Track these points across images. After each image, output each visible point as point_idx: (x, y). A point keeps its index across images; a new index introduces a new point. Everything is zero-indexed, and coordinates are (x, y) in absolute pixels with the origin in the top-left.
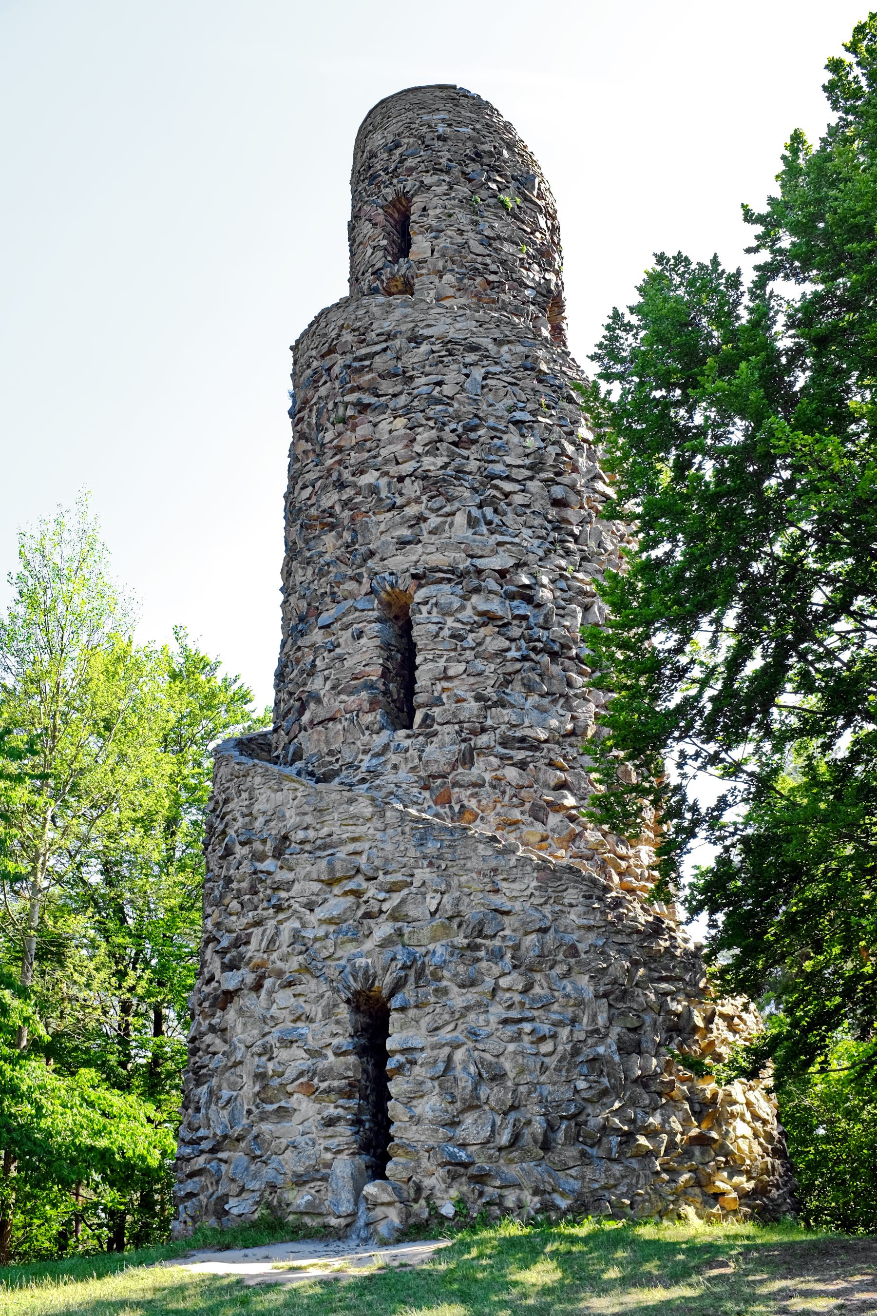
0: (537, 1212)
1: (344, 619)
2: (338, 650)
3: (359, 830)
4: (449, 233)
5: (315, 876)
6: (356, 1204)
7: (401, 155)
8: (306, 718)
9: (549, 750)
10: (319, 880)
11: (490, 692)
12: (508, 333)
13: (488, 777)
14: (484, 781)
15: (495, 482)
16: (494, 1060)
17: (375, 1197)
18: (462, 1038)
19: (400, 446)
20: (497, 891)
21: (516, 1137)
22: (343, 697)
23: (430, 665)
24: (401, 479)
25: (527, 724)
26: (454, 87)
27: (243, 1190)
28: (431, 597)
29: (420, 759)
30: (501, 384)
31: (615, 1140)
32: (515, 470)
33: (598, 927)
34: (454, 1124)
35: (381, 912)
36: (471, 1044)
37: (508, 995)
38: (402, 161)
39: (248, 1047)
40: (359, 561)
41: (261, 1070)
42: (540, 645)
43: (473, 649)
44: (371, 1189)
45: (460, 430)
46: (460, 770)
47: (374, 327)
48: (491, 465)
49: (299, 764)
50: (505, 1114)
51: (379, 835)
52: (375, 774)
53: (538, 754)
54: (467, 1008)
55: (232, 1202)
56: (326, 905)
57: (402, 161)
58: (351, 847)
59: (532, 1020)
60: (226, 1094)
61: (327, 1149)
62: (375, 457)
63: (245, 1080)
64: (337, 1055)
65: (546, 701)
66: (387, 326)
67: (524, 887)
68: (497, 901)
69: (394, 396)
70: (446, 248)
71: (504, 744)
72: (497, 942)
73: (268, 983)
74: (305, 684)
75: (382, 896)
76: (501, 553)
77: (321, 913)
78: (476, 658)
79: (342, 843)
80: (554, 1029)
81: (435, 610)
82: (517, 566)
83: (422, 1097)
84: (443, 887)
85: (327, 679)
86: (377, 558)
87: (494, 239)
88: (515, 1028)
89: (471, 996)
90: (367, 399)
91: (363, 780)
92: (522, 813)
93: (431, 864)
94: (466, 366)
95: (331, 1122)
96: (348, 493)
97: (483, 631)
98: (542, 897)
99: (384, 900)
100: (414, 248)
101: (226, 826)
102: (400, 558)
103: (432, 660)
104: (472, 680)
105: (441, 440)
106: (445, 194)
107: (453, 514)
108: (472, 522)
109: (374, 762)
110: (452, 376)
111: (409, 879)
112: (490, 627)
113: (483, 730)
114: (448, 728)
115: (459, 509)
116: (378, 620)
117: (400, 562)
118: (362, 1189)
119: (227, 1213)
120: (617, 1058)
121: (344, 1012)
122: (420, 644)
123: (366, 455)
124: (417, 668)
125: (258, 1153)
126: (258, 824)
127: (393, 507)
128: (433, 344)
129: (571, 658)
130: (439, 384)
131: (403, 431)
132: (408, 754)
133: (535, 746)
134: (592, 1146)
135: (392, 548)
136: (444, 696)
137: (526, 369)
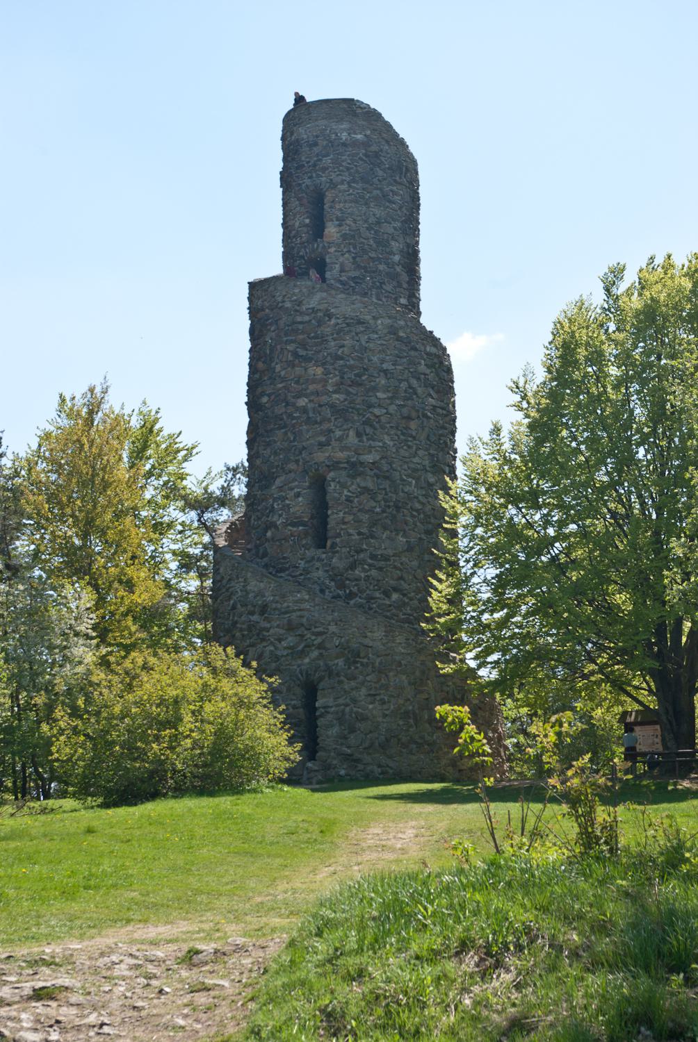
0: (380, 774)
4: (348, 222)
8: (269, 534)
9: (394, 561)
11: (364, 530)
13: (363, 575)
15: (371, 410)
20: (366, 637)
22: (290, 528)
23: (335, 516)
24: (320, 406)
26: (353, 100)
35: (313, 645)
36: (352, 705)
37: (369, 684)
40: (297, 453)
42: (392, 504)
44: (309, 765)
45: (353, 377)
47: (304, 302)
49: (265, 559)
51: (312, 609)
58: (299, 613)
62: (305, 390)
64: (293, 708)
68: (366, 641)
71: (371, 558)
72: (365, 660)
74: (268, 517)
75: (313, 638)
77: (284, 644)
79: (294, 611)
82: (382, 458)
89: (353, 684)
90: (301, 352)
91: (301, 575)
93: (336, 624)
96: (290, 409)
100: (326, 231)
101: (232, 594)
102: (319, 454)
104: (356, 524)
105: (342, 384)
108: (359, 435)
109: (307, 565)
110: (348, 342)
112: (366, 494)
113: (362, 551)
114: (344, 550)
115: (351, 427)
116: (309, 487)
117: (321, 456)
121: (298, 691)
122: (330, 504)
126: (251, 595)
127: (316, 422)
128: (338, 318)
133: (386, 558)
135: (316, 448)
136: (342, 532)
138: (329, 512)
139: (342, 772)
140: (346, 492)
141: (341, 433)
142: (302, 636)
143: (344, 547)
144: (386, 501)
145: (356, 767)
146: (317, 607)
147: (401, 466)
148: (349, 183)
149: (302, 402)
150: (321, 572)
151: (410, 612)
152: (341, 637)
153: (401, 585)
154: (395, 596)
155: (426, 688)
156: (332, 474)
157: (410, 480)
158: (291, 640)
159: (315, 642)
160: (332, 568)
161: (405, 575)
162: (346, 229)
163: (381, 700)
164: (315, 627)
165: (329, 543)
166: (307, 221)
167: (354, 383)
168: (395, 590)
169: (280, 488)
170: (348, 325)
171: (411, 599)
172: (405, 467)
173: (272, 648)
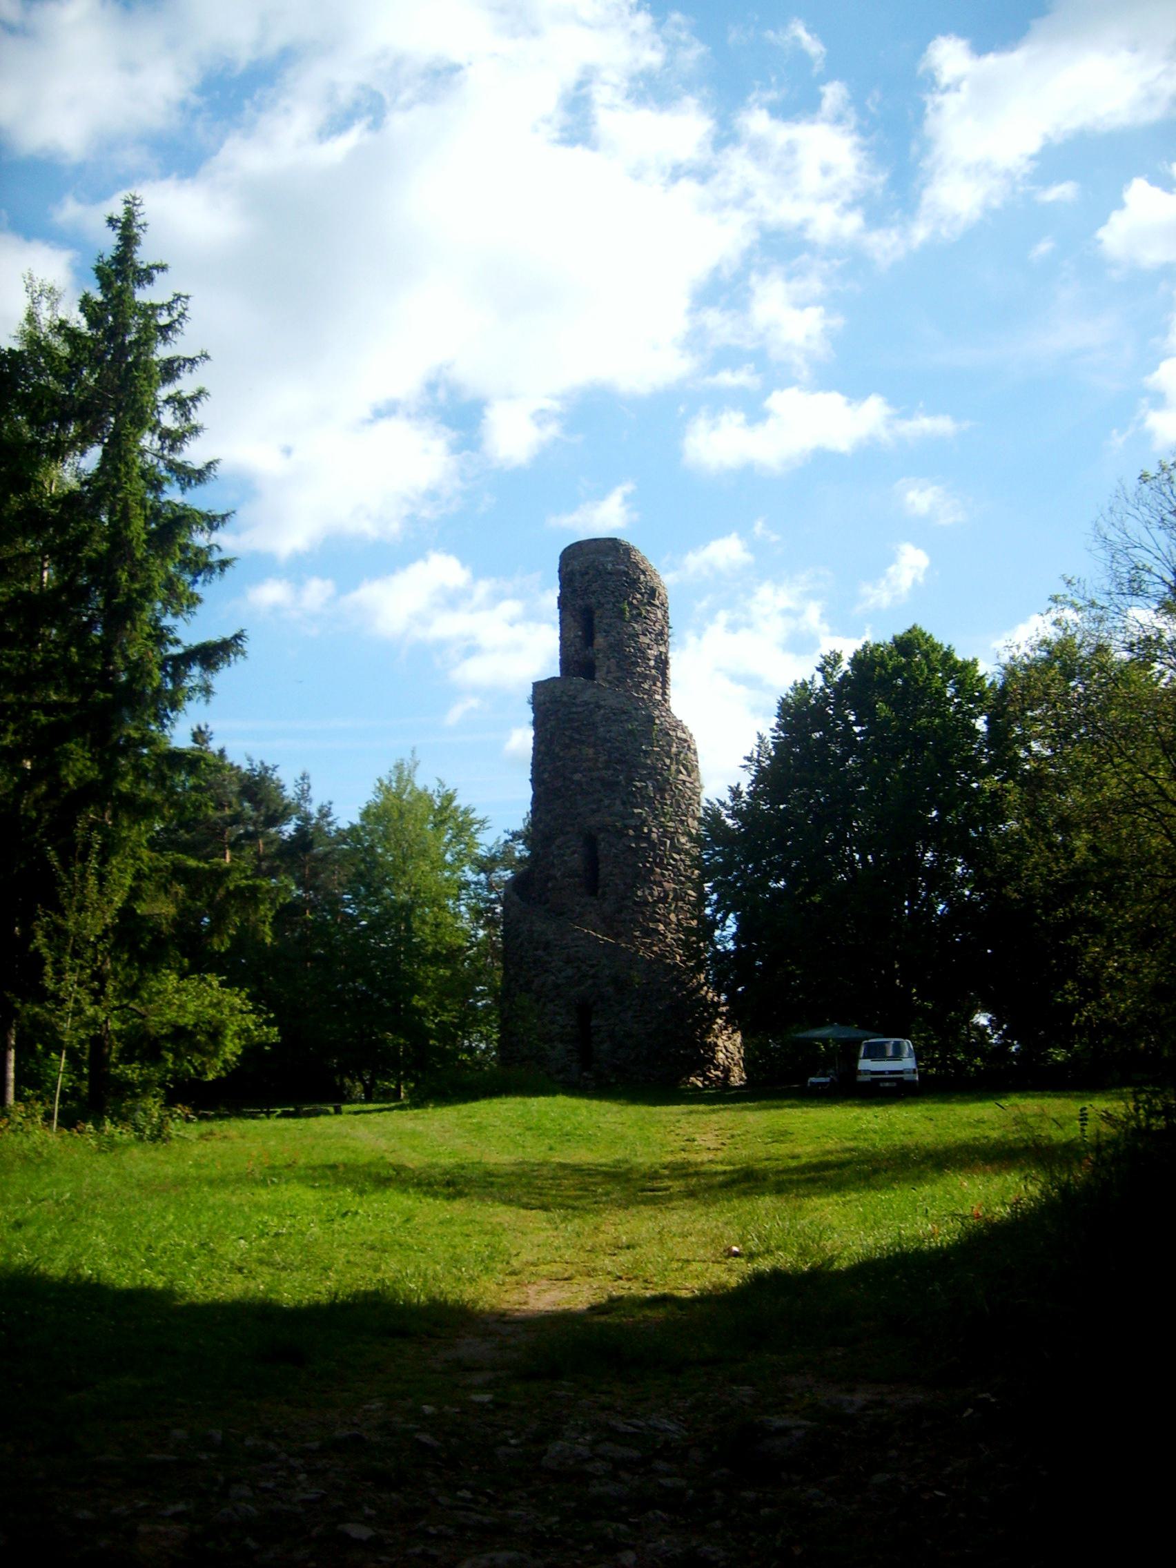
8: (550, 885)
13: (628, 918)
44: (585, 1074)
49: (548, 906)
58: (576, 949)
73: (543, 999)
77: (563, 974)
94: (621, 722)
95: (570, 1051)
108: (624, 803)
126: (535, 935)
138: (600, 866)
142: (578, 968)
149: (577, 777)
156: (602, 836)
158: (570, 971)
159: (591, 972)
162: (611, 639)
165: (600, 891)
166: (580, 633)
167: (619, 762)
169: (559, 847)
170: (614, 714)
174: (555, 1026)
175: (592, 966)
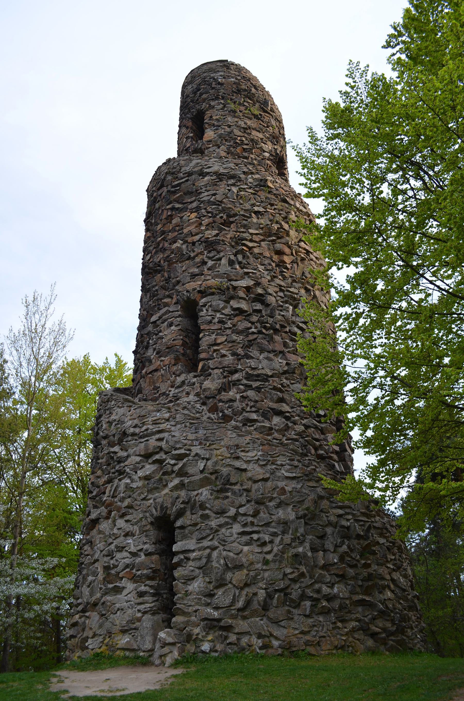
0: (260, 648)
1: (164, 317)
2: (161, 334)
3: (162, 426)
4: (223, 127)
5: (138, 453)
6: (154, 643)
7: (200, 93)
9: (273, 381)
10: (139, 455)
11: (240, 351)
12: (251, 169)
13: (238, 396)
14: (236, 399)
15: (243, 242)
16: (235, 556)
17: (165, 639)
18: (216, 544)
19: (193, 227)
20: (238, 458)
21: (248, 603)
22: (163, 358)
23: (207, 338)
24: (194, 244)
25: (260, 367)
26: (227, 61)
27: (94, 635)
28: (208, 302)
29: (201, 387)
30: (247, 194)
31: (308, 604)
32: (254, 236)
33: (298, 477)
34: (211, 595)
35: (173, 472)
36: (221, 548)
38: (200, 96)
39: (101, 551)
41: (106, 564)
43: (230, 328)
44: (162, 635)
46: (223, 393)
48: (241, 234)
49: (139, 396)
50: (242, 589)
52: (176, 398)
53: (267, 383)
54: (220, 526)
55: (90, 641)
56: (144, 469)
57: (200, 96)
58: (157, 436)
59: (258, 532)
60: (90, 578)
61: (139, 611)
63: (99, 570)
64: (146, 555)
65: (271, 355)
66: (187, 169)
67: (254, 455)
68: (237, 464)
69: (191, 202)
70: (222, 134)
73: (113, 513)
74: (144, 354)
75: (173, 462)
76: (247, 278)
77: (140, 473)
78: (232, 333)
80: (272, 537)
81: (210, 309)
83: (193, 579)
84: (207, 456)
85: (154, 349)
86: (181, 284)
87: (246, 129)
88: (248, 537)
89: (222, 520)
90: (177, 206)
91: (171, 401)
92: (258, 416)
93: (200, 444)
95: (141, 594)
97: (236, 319)
98: (265, 460)
99: (175, 465)
100: (206, 135)
103: (208, 335)
104: (230, 345)
105: (214, 222)
106: (221, 109)
107: (220, 259)
108: (231, 263)
109: (176, 391)
111: (188, 452)
113: (236, 371)
114: (216, 371)
115: (223, 256)
117: (191, 285)
118: (158, 635)
119: (87, 648)
120: (309, 554)
122: (202, 327)
123: (177, 233)
124: (200, 339)
125: (104, 612)
127: (189, 258)
128: (212, 176)
129: (286, 332)
130: (214, 195)
131: (195, 219)
132: (195, 386)
133: (265, 378)
134: (294, 608)
137: (261, 186)
138: (201, 335)
139: (206, 647)
140: (218, 315)
141: (213, 262)
143: (216, 368)
144: (262, 323)
145: (226, 638)
146: (179, 426)
147: (276, 292)
148: (223, 104)
150: (192, 397)
151: (295, 437)
152: (208, 460)
153: (283, 406)
154: (276, 420)
155: (319, 522)
156: (204, 300)
157: (287, 305)
158: (149, 469)
159: (176, 468)
160: (205, 390)
161: (286, 396)
162: (221, 131)
163: (259, 539)
164: (176, 449)
168: (279, 413)
171: (295, 423)
172: (281, 294)
173: (128, 481)
174: (125, 554)
175: (180, 457)
